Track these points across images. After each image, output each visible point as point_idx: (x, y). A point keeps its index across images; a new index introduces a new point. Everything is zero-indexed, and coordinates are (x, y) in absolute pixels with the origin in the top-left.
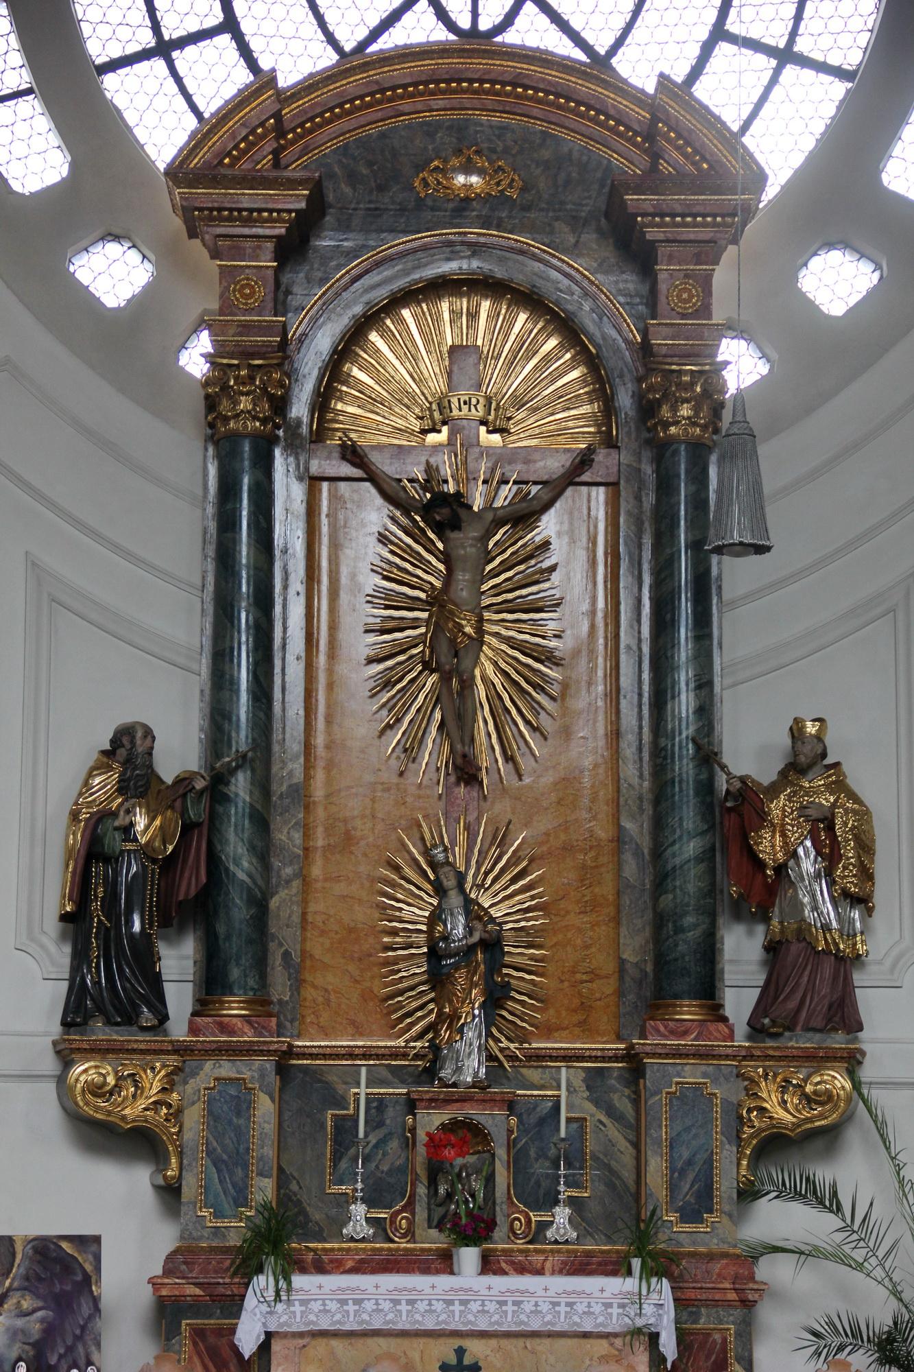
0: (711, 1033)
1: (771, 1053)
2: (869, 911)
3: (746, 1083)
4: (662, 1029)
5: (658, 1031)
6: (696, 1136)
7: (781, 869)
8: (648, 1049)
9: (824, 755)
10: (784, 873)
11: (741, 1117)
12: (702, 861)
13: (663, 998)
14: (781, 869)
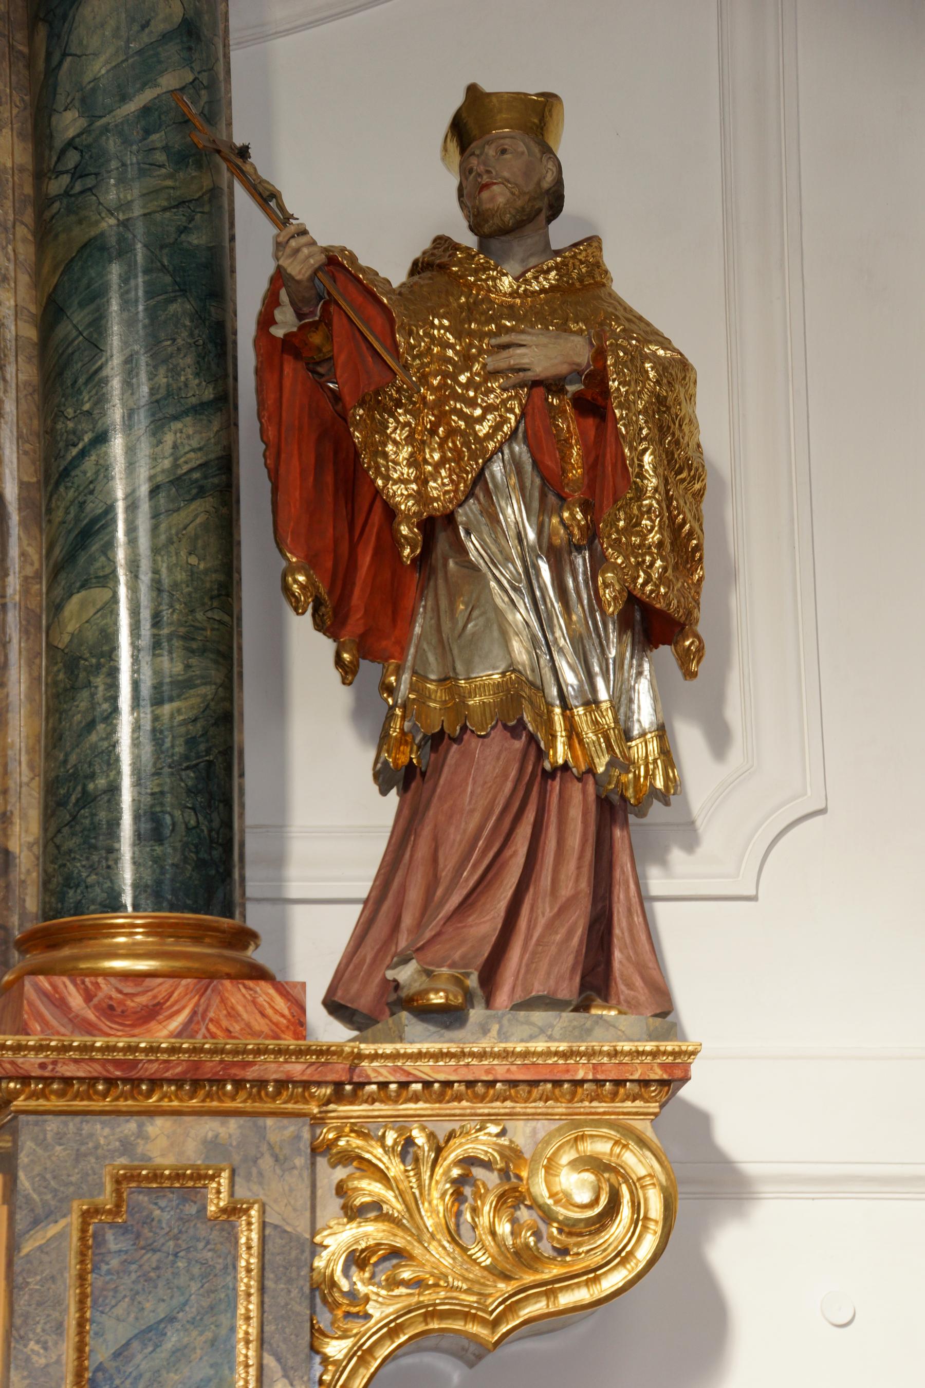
0: (233, 1014)
1: (425, 1069)
2: (687, 663)
3: (340, 1173)
4: (76, 1001)
5: (60, 1004)
6: (180, 1354)
7: (437, 527)
8: (31, 1062)
9: (554, 201)
10: (442, 544)
11: (321, 1289)
12: (202, 492)
13: (78, 910)
14: (437, 527)
